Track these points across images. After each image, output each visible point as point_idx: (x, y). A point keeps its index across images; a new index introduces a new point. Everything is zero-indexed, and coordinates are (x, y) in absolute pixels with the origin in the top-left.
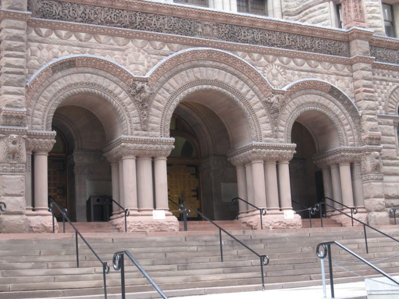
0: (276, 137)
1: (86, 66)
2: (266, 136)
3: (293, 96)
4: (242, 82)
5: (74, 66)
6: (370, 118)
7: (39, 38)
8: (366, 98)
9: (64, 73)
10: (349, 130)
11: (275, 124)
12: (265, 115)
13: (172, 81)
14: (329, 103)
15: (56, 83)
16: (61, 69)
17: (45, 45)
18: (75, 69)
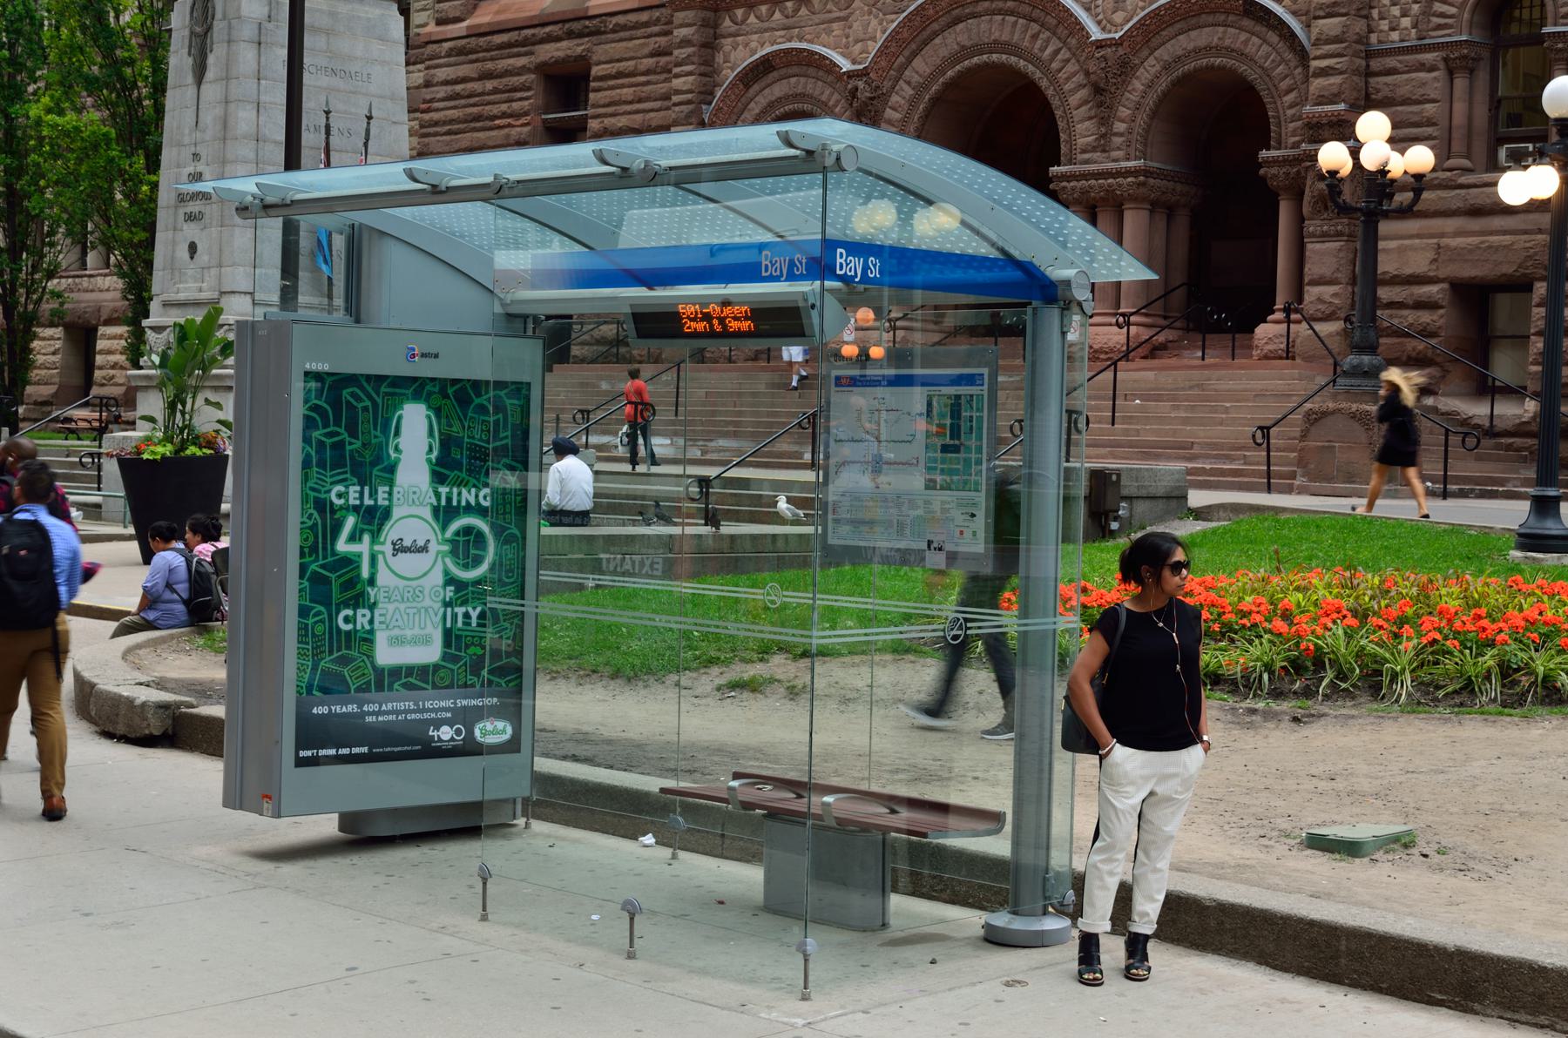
0: (1104, 151)
1: (788, 65)
2: (1084, 151)
3: (1155, 41)
4: (1048, 34)
5: (774, 69)
6: (1322, 69)
7: (734, 28)
8: (1322, 13)
9: (762, 83)
10: (1291, 107)
11: (1105, 121)
12: (1086, 102)
13: (918, 63)
14: (1246, 42)
15: (752, 105)
16: (756, 79)
17: (740, 38)
18: (775, 74)
